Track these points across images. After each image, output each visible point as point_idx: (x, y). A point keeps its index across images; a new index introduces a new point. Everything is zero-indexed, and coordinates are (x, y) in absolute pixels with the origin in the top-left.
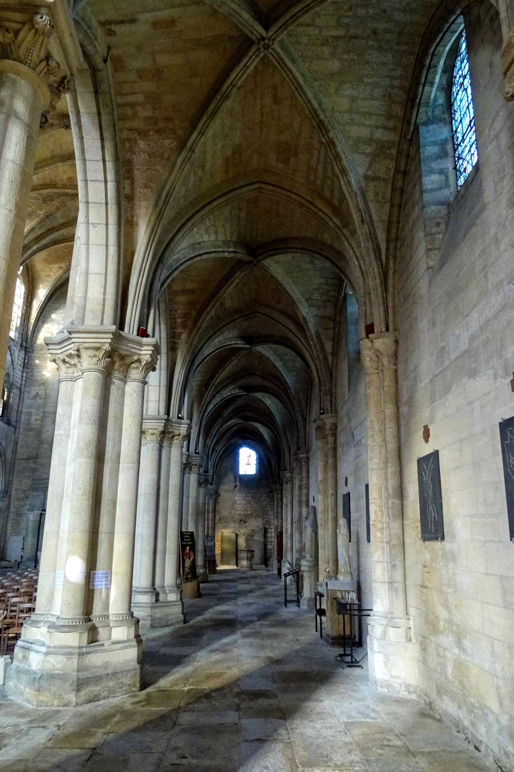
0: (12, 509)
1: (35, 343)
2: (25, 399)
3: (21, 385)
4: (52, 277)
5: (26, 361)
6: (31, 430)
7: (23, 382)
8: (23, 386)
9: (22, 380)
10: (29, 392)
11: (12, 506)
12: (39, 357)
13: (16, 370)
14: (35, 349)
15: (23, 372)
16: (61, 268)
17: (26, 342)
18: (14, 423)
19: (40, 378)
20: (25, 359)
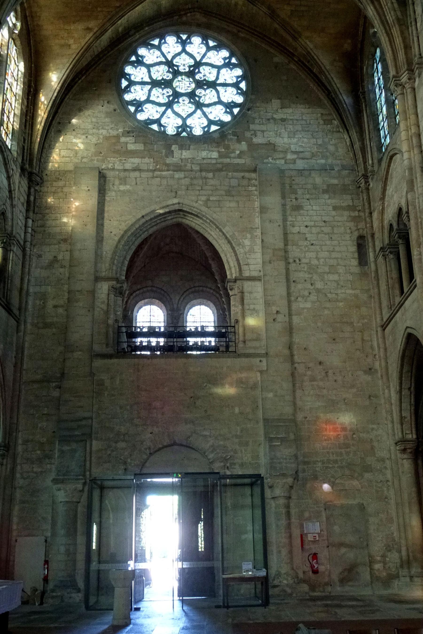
0: (20, 482)
1: (45, 168)
2: (32, 270)
3: (25, 242)
4: (74, 47)
5: (32, 198)
6: (47, 326)
7: (29, 235)
8: (28, 244)
9: (25, 233)
10: (40, 256)
11: (18, 475)
12: (54, 193)
13: (16, 210)
14: (45, 177)
15: (27, 218)
16: (88, 29)
17: (31, 164)
18: (16, 312)
19: (58, 230)
20: (29, 195)
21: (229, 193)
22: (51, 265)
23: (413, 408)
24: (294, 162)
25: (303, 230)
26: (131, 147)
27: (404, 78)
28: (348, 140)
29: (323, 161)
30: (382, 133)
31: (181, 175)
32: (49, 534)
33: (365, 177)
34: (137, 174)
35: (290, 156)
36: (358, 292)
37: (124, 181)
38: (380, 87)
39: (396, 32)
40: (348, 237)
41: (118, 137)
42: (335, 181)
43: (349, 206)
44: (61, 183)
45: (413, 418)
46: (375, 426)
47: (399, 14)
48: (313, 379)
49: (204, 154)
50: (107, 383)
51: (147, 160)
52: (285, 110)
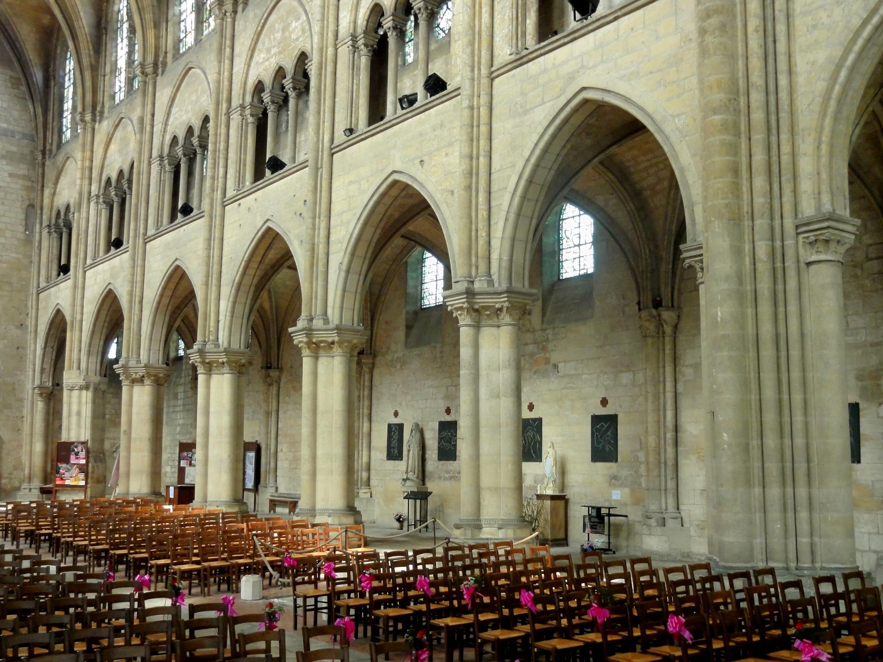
23: (53, 362)
27: (88, 117)
28: (32, 110)
30: (64, 120)
33: (43, 153)
36: (21, 256)
38: (69, 79)
40: (19, 204)
42: (14, 149)
43: (24, 175)
45: (52, 369)
46: (18, 373)
47: (93, 60)
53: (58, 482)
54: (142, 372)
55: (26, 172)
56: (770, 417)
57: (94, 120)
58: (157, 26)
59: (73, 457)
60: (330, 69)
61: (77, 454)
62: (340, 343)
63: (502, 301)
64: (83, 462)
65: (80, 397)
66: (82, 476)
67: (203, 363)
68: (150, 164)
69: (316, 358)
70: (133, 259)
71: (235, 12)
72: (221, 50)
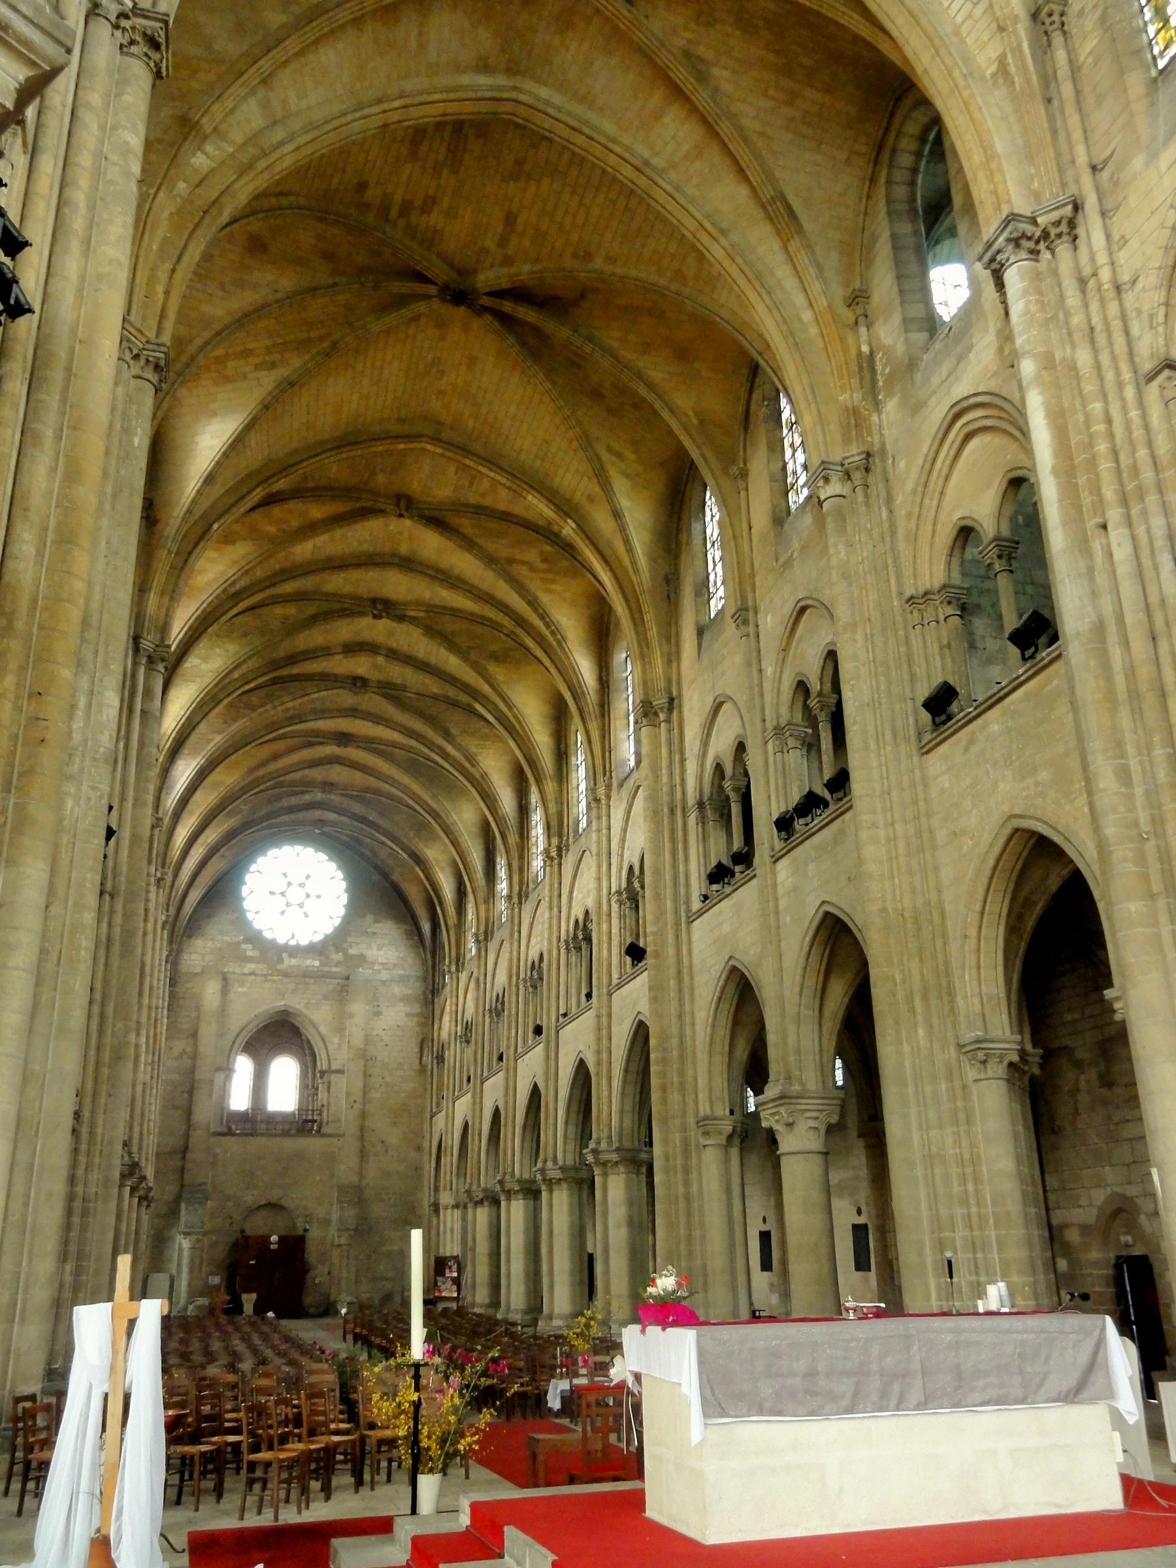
21: (326, 998)
22: (181, 1056)
24: (379, 972)
25: (381, 1032)
26: (250, 953)
27: (453, 968)
29: (402, 972)
31: (286, 980)
32: (174, 1272)
34: (252, 978)
35: (376, 967)
37: (242, 985)
39: (452, 933)
41: (238, 944)
42: (410, 992)
44: (189, 985)
48: (376, 1154)
49: (308, 962)
50: (221, 1156)
51: (261, 966)
52: (377, 925)
53: (437, 1294)
54: (481, 1196)
55: (419, 1011)
56: (683, 1247)
57: (458, 970)
58: (486, 902)
59: (447, 1271)
60: (554, 966)
61: (450, 1267)
62: (565, 1179)
63: (614, 1157)
64: (455, 1275)
65: (453, 1216)
66: (455, 1288)
67: (503, 1191)
68: (484, 1016)
69: (551, 1191)
70: (473, 1097)
71: (520, 903)
72: (512, 935)
